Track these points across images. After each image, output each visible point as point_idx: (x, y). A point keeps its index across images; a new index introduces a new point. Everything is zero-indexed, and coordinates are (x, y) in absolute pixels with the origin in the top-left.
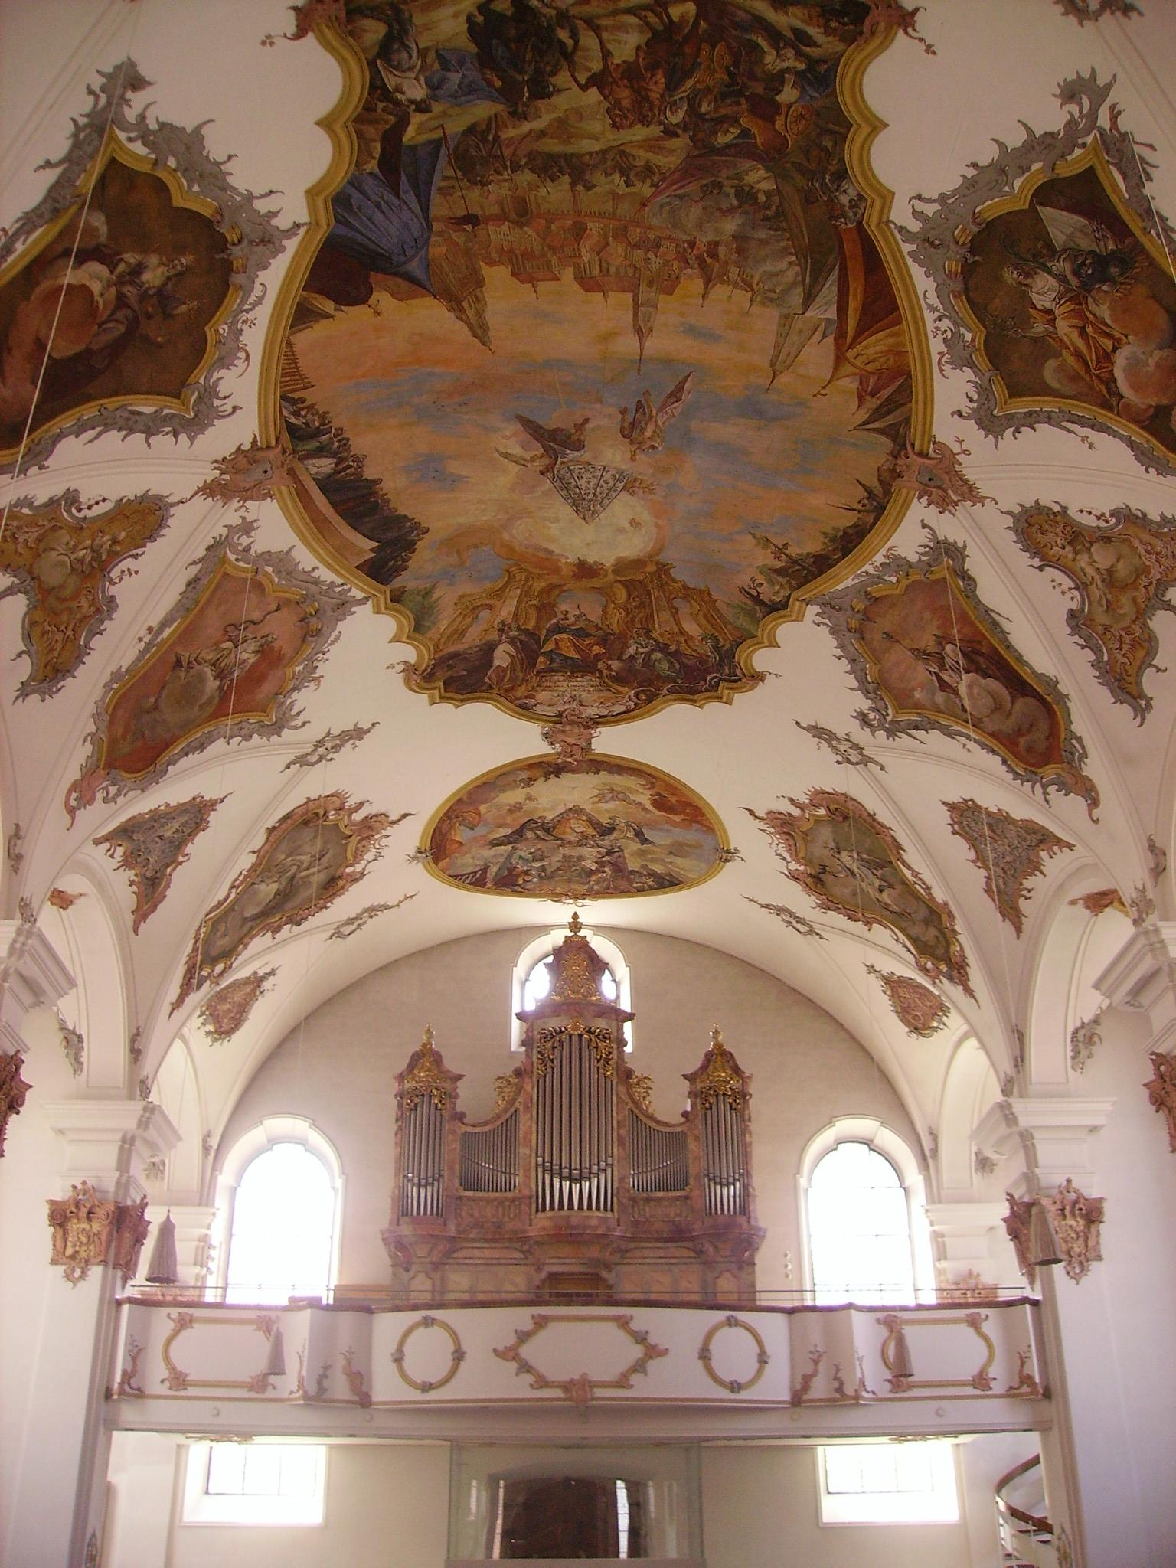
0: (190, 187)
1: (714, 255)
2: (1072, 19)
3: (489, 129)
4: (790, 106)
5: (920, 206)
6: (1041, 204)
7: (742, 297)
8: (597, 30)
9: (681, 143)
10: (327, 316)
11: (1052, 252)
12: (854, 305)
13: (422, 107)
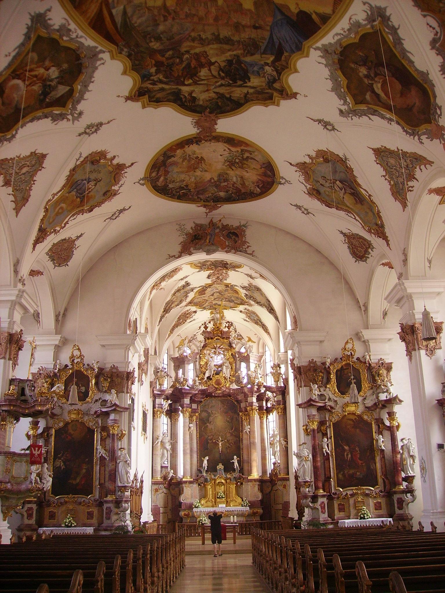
0: (341, 81)
1: (165, 16)
2: (89, 124)
3: (247, 53)
4: (152, 67)
5: (102, 61)
6: (70, 89)
7: (150, 4)
8: (213, 75)
9: (183, 50)
10: (316, 14)
11: (59, 83)
12: (108, 19)
13: (267, 64)
